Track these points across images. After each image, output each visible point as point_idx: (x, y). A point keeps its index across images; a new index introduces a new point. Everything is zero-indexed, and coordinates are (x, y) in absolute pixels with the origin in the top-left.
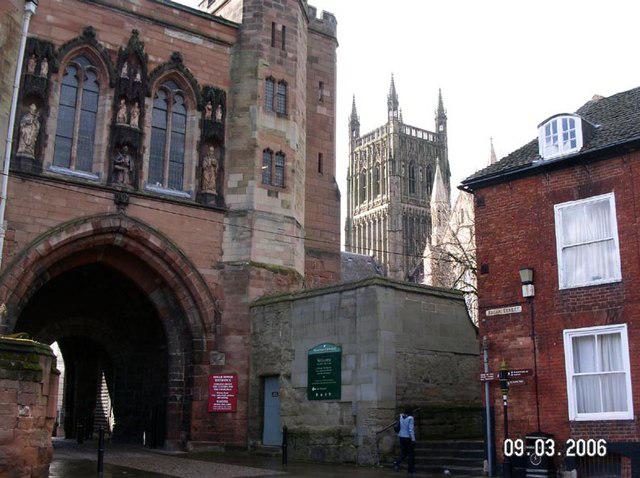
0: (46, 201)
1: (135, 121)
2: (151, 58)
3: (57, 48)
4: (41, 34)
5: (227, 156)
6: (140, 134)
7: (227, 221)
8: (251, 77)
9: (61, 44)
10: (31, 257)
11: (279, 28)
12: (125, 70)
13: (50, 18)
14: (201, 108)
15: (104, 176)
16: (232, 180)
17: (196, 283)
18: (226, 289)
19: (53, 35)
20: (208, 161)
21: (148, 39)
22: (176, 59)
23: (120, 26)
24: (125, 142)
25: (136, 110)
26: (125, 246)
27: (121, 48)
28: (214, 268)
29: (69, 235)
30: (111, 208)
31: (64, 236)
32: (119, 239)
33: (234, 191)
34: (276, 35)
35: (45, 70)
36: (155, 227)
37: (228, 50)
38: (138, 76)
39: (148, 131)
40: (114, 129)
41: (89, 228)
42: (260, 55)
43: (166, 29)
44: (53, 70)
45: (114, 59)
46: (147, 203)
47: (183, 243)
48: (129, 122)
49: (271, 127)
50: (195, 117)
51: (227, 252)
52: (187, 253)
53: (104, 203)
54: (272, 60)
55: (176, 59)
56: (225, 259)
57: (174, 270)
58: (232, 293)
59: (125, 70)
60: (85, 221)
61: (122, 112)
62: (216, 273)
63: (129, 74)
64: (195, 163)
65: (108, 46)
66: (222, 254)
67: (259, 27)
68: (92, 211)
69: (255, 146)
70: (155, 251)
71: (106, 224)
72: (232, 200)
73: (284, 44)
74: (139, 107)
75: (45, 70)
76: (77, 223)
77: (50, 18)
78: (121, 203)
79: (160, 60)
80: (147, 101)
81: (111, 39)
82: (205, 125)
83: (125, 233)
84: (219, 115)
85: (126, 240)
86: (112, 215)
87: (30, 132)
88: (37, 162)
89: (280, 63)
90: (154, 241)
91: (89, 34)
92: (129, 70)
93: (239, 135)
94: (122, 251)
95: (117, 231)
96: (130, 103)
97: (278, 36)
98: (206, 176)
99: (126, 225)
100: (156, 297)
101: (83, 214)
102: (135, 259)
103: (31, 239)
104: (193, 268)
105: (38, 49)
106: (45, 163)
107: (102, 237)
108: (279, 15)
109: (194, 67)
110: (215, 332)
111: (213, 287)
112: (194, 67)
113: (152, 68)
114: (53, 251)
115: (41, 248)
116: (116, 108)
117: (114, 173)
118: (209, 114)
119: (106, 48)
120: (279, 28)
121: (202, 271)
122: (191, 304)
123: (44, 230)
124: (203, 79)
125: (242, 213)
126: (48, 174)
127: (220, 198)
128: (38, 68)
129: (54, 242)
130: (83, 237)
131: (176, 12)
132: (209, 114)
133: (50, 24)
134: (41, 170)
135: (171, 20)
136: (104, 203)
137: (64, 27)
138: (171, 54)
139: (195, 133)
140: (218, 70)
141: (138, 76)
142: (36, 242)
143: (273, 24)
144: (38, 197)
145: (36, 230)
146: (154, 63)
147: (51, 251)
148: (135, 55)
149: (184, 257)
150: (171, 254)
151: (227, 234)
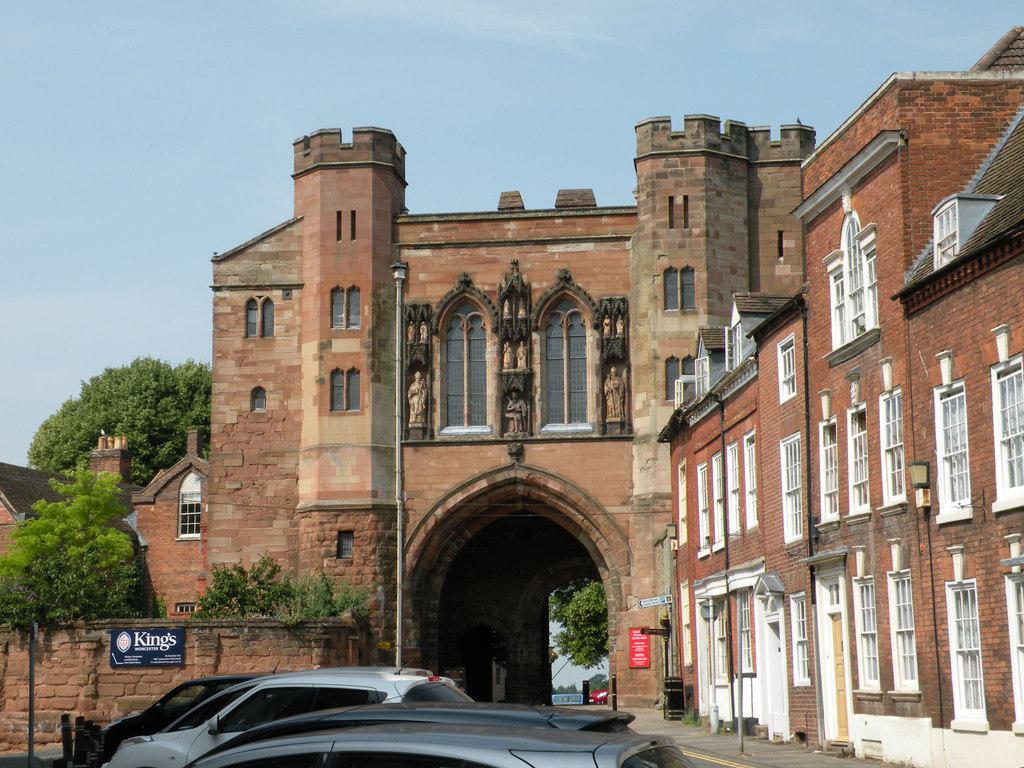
0: (440, 466)
1: (521, 363)
2: (535, 285)
3: (434, 306)
4: (414, 296)
5: (633, 374)
6: (529, 377)
7: (635, 448)
8: (647, 275)
9: (438, 300)
10: (431, 523)
11: (679, 200)
12: (506, 310)
13: (422, 276)
14: (598, 327)
15: (497, 427)
16: (638, 400)
17: (601, 520)
18: (636, 527)
19: (428, 294)
20: (610, 384)
21: (529, 266)
22: (566, 278)
23: (494, 261)
24: (516, 389)
25: (521, 350)
26: (529, 494)
27: (501, 288)
28: (624, 504)
29: (465, 496)
30: (507, 460)
31: (460, 497)
32: (521, 489)
33: (640, 414)
34: (675, 212)
35: (424, 335)
36: (552, 471)
37: (628, 245)
38: (522, 313)
39: (537, 368)
40: (500, 375)
41: (483, 484)
42: (655, 246)
43: (548, 246)
44: (432, 332)
45: (495, 301)
46: (541, 447)
47: (587, 483)
48: (515, 366)
49: (673, 330)
50: (591, 337)
51: (637, 483)
52: (592, 492)
53: (499, 456)
54: (670, 246)
55: (566, 278)
56: (636, 492)
57: (581, 514)
58: (639, 531)
59: (506, 310)
60: (479, 478)
61: (507, 358)
62: (625, 509)
63: (511, 313)
64: (596, 390)
65: (486, 288)
66: (632, 487)
67: (654, 208)
68: (486, 467)
69: (656, 358)
70: (560, 496)
71: (500, 477)
72: (641, 425)
73: (686, 221)
74: (525, 345)
75: (424, 335)
76: (470, 483)
77: (422, 276)
78: (518, 454)
79: (545, 284)
80: (535, 336)
81: (489, 280)
82: (603, 344)
83: (523, 482)
84: (620, 328)
85: (528, 488)
86: (506, 468)
87: (416, 403)
88: (427, 430)
89: (681, 246)
90: (553, 485)
91: (467, 282)
92: (510, 308)
93: (640, 347)
94: (526, 499)
95: (514, 482)
96: (515, 344)
97: (679, 213)
98: (610, 403)
99: (522, 474)
100: (582, 538)
101: (477, 472)
102: (539, 501)
103: (429, 507)
104: (598, 506)
105: (417, 315)
106: (436, 428)
107: (502, 490)
108: (678, 185)
109: (588, 279)
110: (629, 574)
111: (624, 525)
112: (588, 279)
113: (536, 297)
114: (452, 513)
115: (439, 512)
116: (501, 354)
117: (504, 424)
118: (607, 330)
119: (484, 291)
120: (679, 200)
121: (610, 510)
122: (606, 546)
123: (441, 495)
124: (596, 291)
125: (645, 439)
126: (438, 438)
127: (626, 425)
128: (418, 334)
129: (451, 503)
130: (482, 493)
131: (560, 221)
132: (607, 330)
133: (424, 283)
134: (432, 436)
135: (556, 233)
136: (499, 456)
137: (440, 282)
138: (557, 273)
139: (592, 356)
140: (616, 274)
141: (522, 313)
142: (436, 507)
143: (671, 199)
144: (433, 463)
145: (433, 497)
146: (539, 289)
147: (450, 514)
148: (516, 292)
149: (587, 498)
150: (573, 497)
151: (636, 464)
